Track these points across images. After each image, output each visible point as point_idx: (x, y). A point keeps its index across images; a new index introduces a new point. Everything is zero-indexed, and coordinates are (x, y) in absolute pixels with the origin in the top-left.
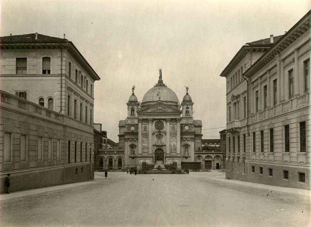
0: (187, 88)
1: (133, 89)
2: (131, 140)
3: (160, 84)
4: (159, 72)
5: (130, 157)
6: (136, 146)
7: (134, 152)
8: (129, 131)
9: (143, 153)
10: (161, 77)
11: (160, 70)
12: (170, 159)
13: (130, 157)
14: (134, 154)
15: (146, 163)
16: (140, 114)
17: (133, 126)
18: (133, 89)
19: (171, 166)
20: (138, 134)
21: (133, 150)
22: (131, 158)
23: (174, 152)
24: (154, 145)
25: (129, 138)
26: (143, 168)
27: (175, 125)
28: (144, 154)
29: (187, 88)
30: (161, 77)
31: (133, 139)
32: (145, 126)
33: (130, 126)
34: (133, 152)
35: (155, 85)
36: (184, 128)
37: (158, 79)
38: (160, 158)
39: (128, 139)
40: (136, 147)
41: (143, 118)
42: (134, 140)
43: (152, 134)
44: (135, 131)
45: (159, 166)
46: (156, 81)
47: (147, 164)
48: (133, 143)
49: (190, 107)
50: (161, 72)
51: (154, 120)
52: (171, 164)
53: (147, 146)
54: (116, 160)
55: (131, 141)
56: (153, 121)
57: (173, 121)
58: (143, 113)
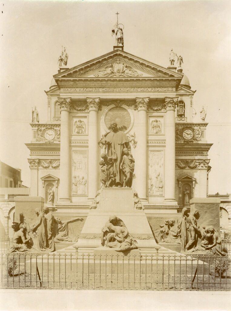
2: (46, 165)
6: (59, 180)
7: (53, 196)
8: (41, 142)
9: (74, 196)
14: (53, 200)
16: (63, 83)
21: (51, 191)
23: (158, 193)
26: (20, 233)
31: (51, 162)
32: (81, 121)
33: (43, 128)
36: (182, 133)
38: (122, 172)
39: (39, 163)
40: (58, 183)
42: (54, 165)
43: (99, 143)
44: (55, 142)
45: (116, 222)
48: (51, 172)
51: (103, 103)
53: (83, 178)
54: (8, 218)
55: (46, 168)
56: (100, 109)
57: (156, 108)
58: (74, 81)
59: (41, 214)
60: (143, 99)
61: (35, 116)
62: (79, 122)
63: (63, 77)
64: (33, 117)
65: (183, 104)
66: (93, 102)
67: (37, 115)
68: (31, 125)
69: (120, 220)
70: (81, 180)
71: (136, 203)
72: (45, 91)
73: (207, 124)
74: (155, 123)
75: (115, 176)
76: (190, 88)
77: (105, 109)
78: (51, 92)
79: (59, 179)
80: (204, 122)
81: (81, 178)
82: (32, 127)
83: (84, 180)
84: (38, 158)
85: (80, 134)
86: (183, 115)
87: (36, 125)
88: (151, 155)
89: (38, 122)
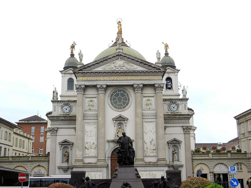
0: (167, 46)
1: (73, 47)
3: (120, 43)
4: (118, 25)
5: (60, 168)
10: (120, 32)
11: (120, 22)
12: (146, 171)
13: (60, 168)
15: (84, 173)
17: (67, 105)
18: (73, 47)
19: (165, 183)
20: (75, 120)
22: (61, 170)
24: (108, 142)
25: (58, 128)
27: (152, 99)
28: (87, 161)
29: (167, 46)
30: (120, 32)
34: (65, 159)
35: (111, 45)
37: (115, 36)
41: (86, 84)
46: (114, 38)
47: (88, 179)
49: (172, 76)
50: (121, 25)
52: (163, 178)
53: (94, 144)
59: (85, 181)
60: (138, 85)
61: (55, 94)
62: (90, 101)
63: (79, 70)
64: (53, 95)
65: (171, 80)
66: (101, 87)
67: (57, 94)
68: (52, 101)
69: (129, 184)
70: (92, 145)
71: (136, 174)
72: (60, 71)
73: (188, 99)
74: (148, 102)
75: (125, 159)
76: (176, 67)
77: (109, 91)
78: (65, 71)
79: (73, 143)
80: (184, 98)
81: (92, 143)
82: (53, 103)
83: (94, 145)
84: (57, 127)
85: (91, 111)
86: (171, 88)
87: (56, 102)
88: (145, 124)
89: (57, 99)
